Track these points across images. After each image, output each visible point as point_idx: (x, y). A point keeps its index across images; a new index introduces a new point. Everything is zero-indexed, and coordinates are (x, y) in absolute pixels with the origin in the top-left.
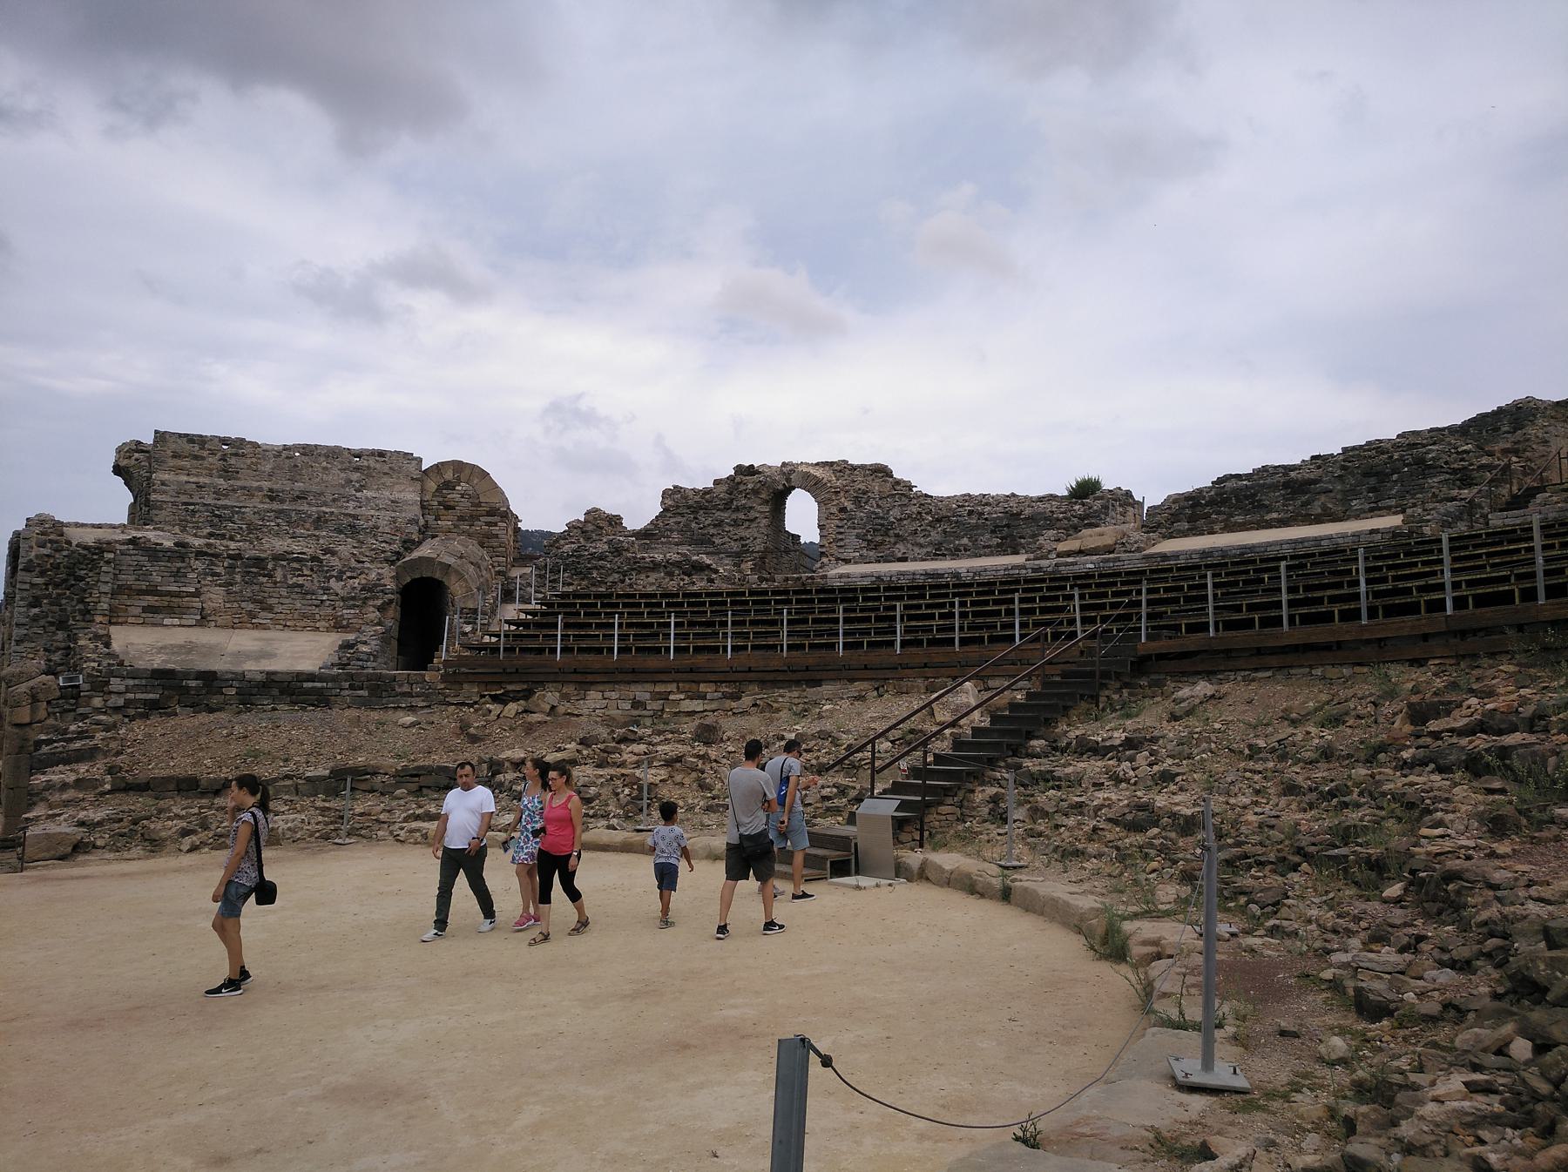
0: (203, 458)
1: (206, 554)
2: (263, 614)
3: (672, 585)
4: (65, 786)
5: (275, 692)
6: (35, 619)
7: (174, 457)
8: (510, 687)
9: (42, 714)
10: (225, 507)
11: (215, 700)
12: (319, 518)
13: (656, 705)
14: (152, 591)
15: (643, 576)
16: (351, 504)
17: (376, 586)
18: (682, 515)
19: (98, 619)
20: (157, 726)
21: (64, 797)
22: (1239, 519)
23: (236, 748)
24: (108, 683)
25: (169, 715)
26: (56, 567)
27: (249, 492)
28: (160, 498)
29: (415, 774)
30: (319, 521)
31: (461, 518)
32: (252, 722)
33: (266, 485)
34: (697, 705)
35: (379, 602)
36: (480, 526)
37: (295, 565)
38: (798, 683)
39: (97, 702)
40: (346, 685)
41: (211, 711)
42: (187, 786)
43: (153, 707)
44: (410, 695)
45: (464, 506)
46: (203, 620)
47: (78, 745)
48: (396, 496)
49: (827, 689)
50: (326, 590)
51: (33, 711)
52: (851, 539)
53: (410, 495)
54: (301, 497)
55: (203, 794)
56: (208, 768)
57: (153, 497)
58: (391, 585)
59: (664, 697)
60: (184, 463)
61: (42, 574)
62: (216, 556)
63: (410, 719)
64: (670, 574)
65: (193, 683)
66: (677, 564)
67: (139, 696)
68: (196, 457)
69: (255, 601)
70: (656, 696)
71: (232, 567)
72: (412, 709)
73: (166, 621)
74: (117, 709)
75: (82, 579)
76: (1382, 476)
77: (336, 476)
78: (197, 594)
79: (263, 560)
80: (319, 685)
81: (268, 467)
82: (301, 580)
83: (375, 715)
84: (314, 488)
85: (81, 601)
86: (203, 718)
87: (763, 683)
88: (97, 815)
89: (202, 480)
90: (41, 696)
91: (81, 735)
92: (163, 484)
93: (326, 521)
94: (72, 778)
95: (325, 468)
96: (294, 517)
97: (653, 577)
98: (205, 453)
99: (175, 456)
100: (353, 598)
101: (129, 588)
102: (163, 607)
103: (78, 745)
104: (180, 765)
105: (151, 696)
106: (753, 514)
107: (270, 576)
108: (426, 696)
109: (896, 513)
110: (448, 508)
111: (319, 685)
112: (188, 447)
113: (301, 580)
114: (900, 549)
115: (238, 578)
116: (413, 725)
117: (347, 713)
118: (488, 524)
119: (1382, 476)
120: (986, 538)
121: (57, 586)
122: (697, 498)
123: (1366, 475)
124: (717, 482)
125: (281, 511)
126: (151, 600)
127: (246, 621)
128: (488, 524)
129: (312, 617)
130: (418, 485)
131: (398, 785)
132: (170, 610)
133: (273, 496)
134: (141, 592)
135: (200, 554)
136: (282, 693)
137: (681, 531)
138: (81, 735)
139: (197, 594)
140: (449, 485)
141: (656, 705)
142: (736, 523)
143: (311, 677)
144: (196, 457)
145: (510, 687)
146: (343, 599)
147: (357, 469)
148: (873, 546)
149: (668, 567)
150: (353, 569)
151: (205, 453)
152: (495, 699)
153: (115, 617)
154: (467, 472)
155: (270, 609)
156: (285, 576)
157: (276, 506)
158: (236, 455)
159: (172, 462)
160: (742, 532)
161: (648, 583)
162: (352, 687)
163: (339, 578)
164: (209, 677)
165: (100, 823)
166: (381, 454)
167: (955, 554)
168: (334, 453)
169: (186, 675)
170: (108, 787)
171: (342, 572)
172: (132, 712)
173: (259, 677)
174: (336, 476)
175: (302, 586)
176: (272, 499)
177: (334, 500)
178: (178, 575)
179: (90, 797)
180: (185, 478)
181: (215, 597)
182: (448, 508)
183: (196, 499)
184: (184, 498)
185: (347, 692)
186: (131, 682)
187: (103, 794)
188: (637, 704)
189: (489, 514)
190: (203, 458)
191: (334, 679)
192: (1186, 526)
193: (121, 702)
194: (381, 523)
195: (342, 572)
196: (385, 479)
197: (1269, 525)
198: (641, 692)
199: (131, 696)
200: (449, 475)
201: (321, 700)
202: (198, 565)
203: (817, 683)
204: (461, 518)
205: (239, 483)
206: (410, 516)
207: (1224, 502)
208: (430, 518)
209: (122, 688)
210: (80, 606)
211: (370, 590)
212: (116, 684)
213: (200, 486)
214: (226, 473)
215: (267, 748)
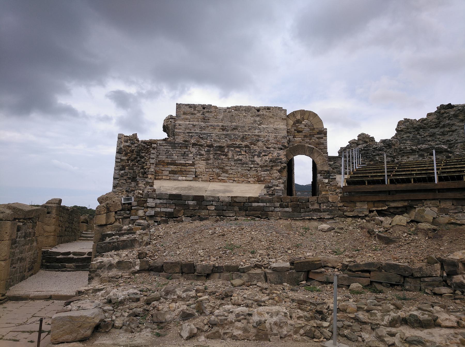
0: (195, 114)
1: (197, 145)
2: (224, 174)
4: (111, 266)
5: (236, 209)
6: (122, 176)
7: (184, 114)
8: (393, 205)
9: (112, 219)
10: (204, 134)
11: (204, 213)
12: (243, 137)
14: (173, 163)
15: (405, 158)
16: (257, 131)
17: (277, 159)
18: (410, 133)
19: (150, 176)
20: (172, 227)
21: (110, 274)
23: (219, 243)
24: (146, 202)
25: (178, 221)
26: (132, 151)
27: (214, 127)
28: (178, 131)
29: (366, 270)
31: (305, 136)
32: (223, 226)
33: (221, 124)
35: (279, 168)
37: (238, 150)
39: (141, 213)
40: (278, 204)
41: (201, 219)
42: (188, 270)
43: (171, 216)
44: (319, 211)
45: (307, 130)
46: (196, 178)
47: (125, 238)
48: (276, 126)
50: (253, 162)
51: (108, 217)
53: (282, 126)
54: (235, 129)
55: (199, 277)
56: (203, 258)
57: (176, 130)
60: (188, 117)
61: (126, 155)
62: (201, 146)
63: (325, 226)
64: (422, 156)
65: (191, 203)
67: (163, 210)
68: (192, 114)
69: (220, 168)
71: (208, 151)
72: (321, 220)
73: (180, 178)
74: (151, 217)
75: (143, 157)
77: (249, 120)
78: (193, 164)
79: (223, 147)
80: (261, 204)
81: (221, 117)
82: (240, 157)
83: (300, 224)
85: (142, 168)
86: (197, 223)
88: (120, 293)
90: (112, 209)
91: (130, 231)
92: (180, 125)
93: (246, 139)
94: (117, 259)
95: (245, 116)
96: (233, 137)
98: (196, 112)
99: (185, 114)
100: (266, 166)
101: (163, 162)
102: (179, 171)
103: (125, 238)
104: (182, 255)
105: (169, 210)
106: (454, 128)
107: (226, 155)
108: (329, 211)
110: (299, 132)
111: (261, 204)
112: (189, 109)
113: (240, 157)
115: (212, 156)
116: (330, 230)
117: (281, 221)
118: (318, 138)
121: (132, 160)
122: (419, 123)
124: (429, 115)
125: (227, 135)
126: (172, 168)
128: (318, 138)
130: (285, 121)
131: (351, 280)
132: (181, 173)
134: (168, 164)
135: (194, 145)
136: (240, 209)
138: (130, 231)
139: (193, 164)
140: (299, 122)
142: (443, 134)
143: (257, 200)
144: (192, 114)
145: (393, 205)
146: (261, 167)
147: (258, 116)
150: (264, 151)
151: (196, 112)
152: (381, 213)
153: (157, 176)
154: (307, 115)
155: (226, 172)
156: (233, 155)
157: (225, 133)
158: (208, 112)
159: (183, 116)
160: (447, 138)
162: (281, 206)
163: (259, 156)
165: (122, 303)
166: (268, 108)
169: (188, 198)
170: (137, 268)
171: (260, 153)
172: (159, 219)
173: (227, 200)
174: (249, 120)
175: (241, 160)
176: (223, 130)
177: (249, 129)
178: (184, 155)
179: (126, 275)
180: (188, 123)
181: (201, 166)
182: (299, 132)
183: (192, 131)
184: (188, 131)
185: (278, 209)
186: (158, 201)
187: (134, 273)
190: (195, 114)
191: (270, 201)
193: (152, 213)
194: (271, 138)
195: (260, 153)
196: (272, 120)
199: (158, 210)
200: (299, 117)
201: (263, 214)
202: (194, 150)
204: (305, 136)
206: (283, 135)
208: (291, 137)
209: (153, 205)
210: (142, 170)
211: (274, 162)
212: (151, 202)
213: (194, 126)
214: (205, 120)
215: (238, 243)
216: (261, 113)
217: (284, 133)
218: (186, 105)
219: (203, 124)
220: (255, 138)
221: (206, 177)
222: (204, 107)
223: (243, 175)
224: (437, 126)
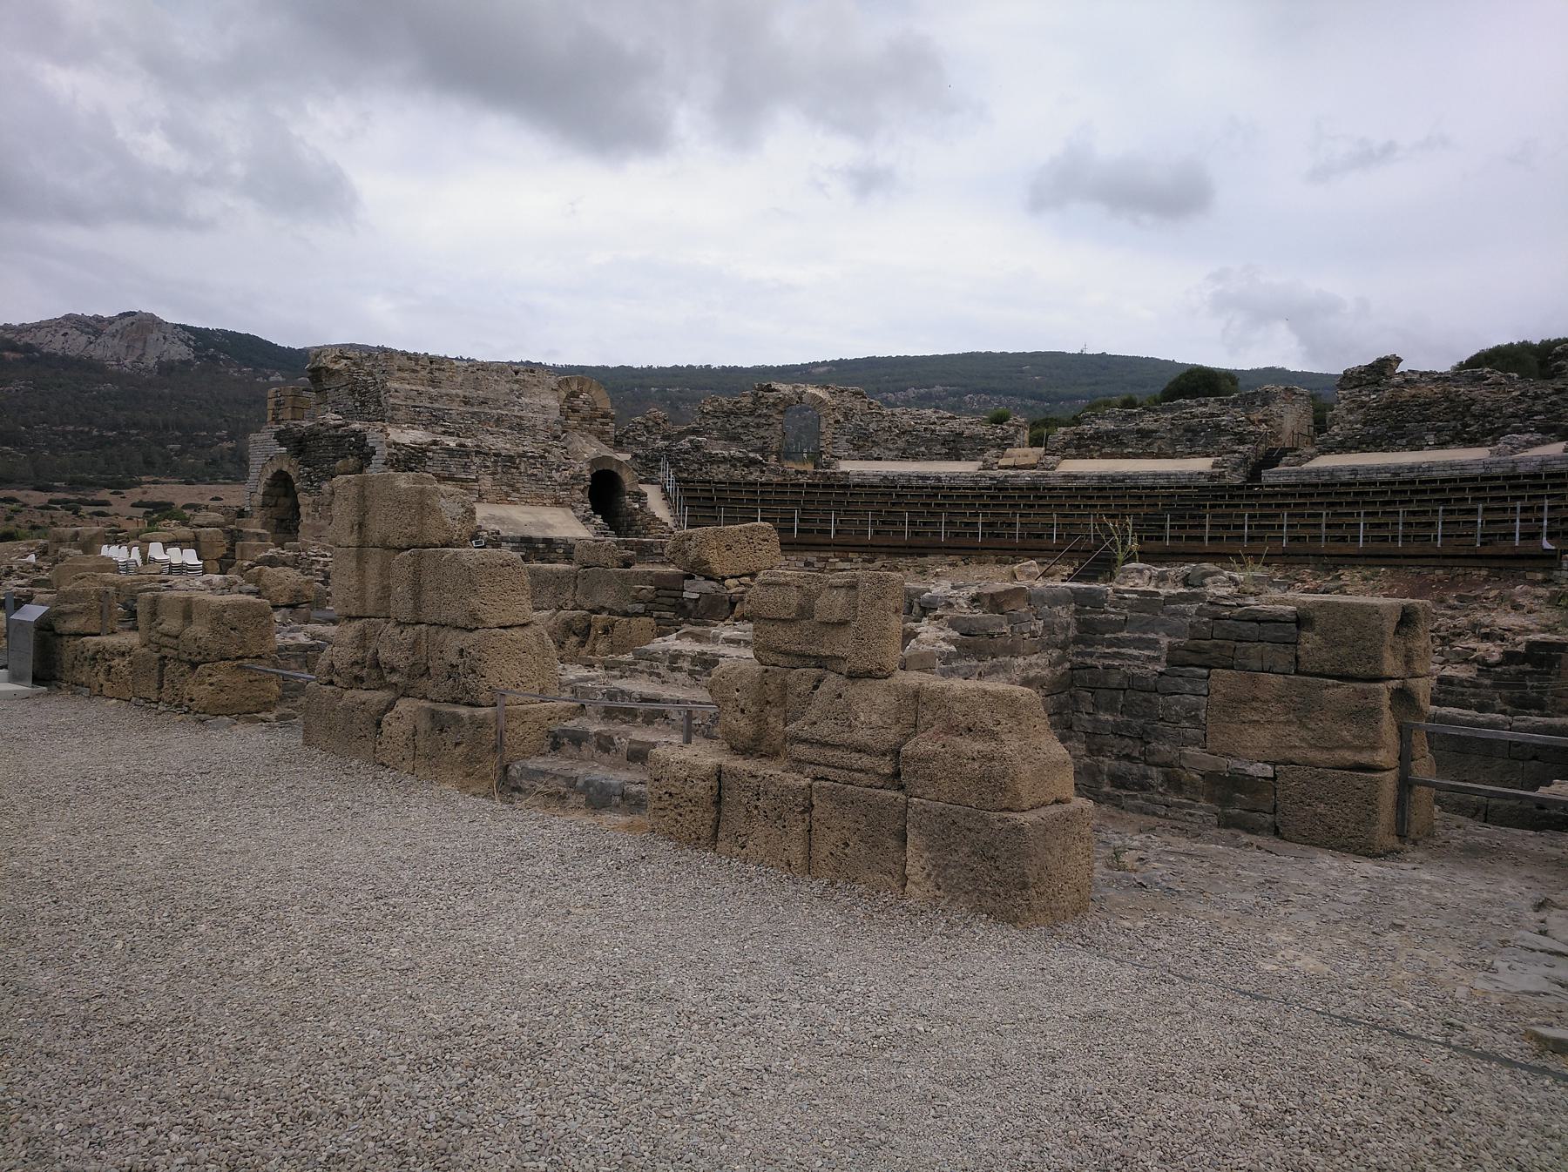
3: (737, 474)
11: (553, 556)
13: (821, 565)
22: (1107, 450)
27: (451, 398)
30: (499, 421)
31: (584, 419)
34: (847, 565)
36: (596, 426)
38: (911, 555)
49: (931, 559)
52: (843, 443)
53: (552, 402)
59: (826, 560)
60: (405, 375)
64: (734, 466)
66: (740, 460)
70: (820, 560)
76: (1195, 433)
77: (504, 387)
78: (476, 480)
84: (491, 396)
87: (889, 554)
89: (421, 388)
97: (722, 468)
106: (771, 420)
109: (873, 426)
110: (574, 411)
112: (408, 363)
114: (876, 451)
119: (1195, 433)
120: (938, 448)
127: (504, 499)
137: (719, 430)
139: (476, 480)
140: (574, 395)
141: (821, 565)
142: (758, 426)
147: (517, 381)
148: (858, 448)
149: (732, 461)
155: (518, 490)
160: (762, 433)
161: (719, 473)
164: (548, 542)
167: (916, 457)
169: (538, 540)
174: (504, 387)
181: (487, 482)
182: (574, 411)
184: (410, 402)
188: (807, 564)
192: (1074, 452)
196: (535, 390)
200: (575, 387)
202: (477, 460)
203: (925, 555)
204: (584, 419)
214: (433, 382)
216: (519, 377)
217: (555, 415)
218: (404, 353)
220: (515, 421)
221: (492, 497)
222: (432, 360)
224: (752, 414)
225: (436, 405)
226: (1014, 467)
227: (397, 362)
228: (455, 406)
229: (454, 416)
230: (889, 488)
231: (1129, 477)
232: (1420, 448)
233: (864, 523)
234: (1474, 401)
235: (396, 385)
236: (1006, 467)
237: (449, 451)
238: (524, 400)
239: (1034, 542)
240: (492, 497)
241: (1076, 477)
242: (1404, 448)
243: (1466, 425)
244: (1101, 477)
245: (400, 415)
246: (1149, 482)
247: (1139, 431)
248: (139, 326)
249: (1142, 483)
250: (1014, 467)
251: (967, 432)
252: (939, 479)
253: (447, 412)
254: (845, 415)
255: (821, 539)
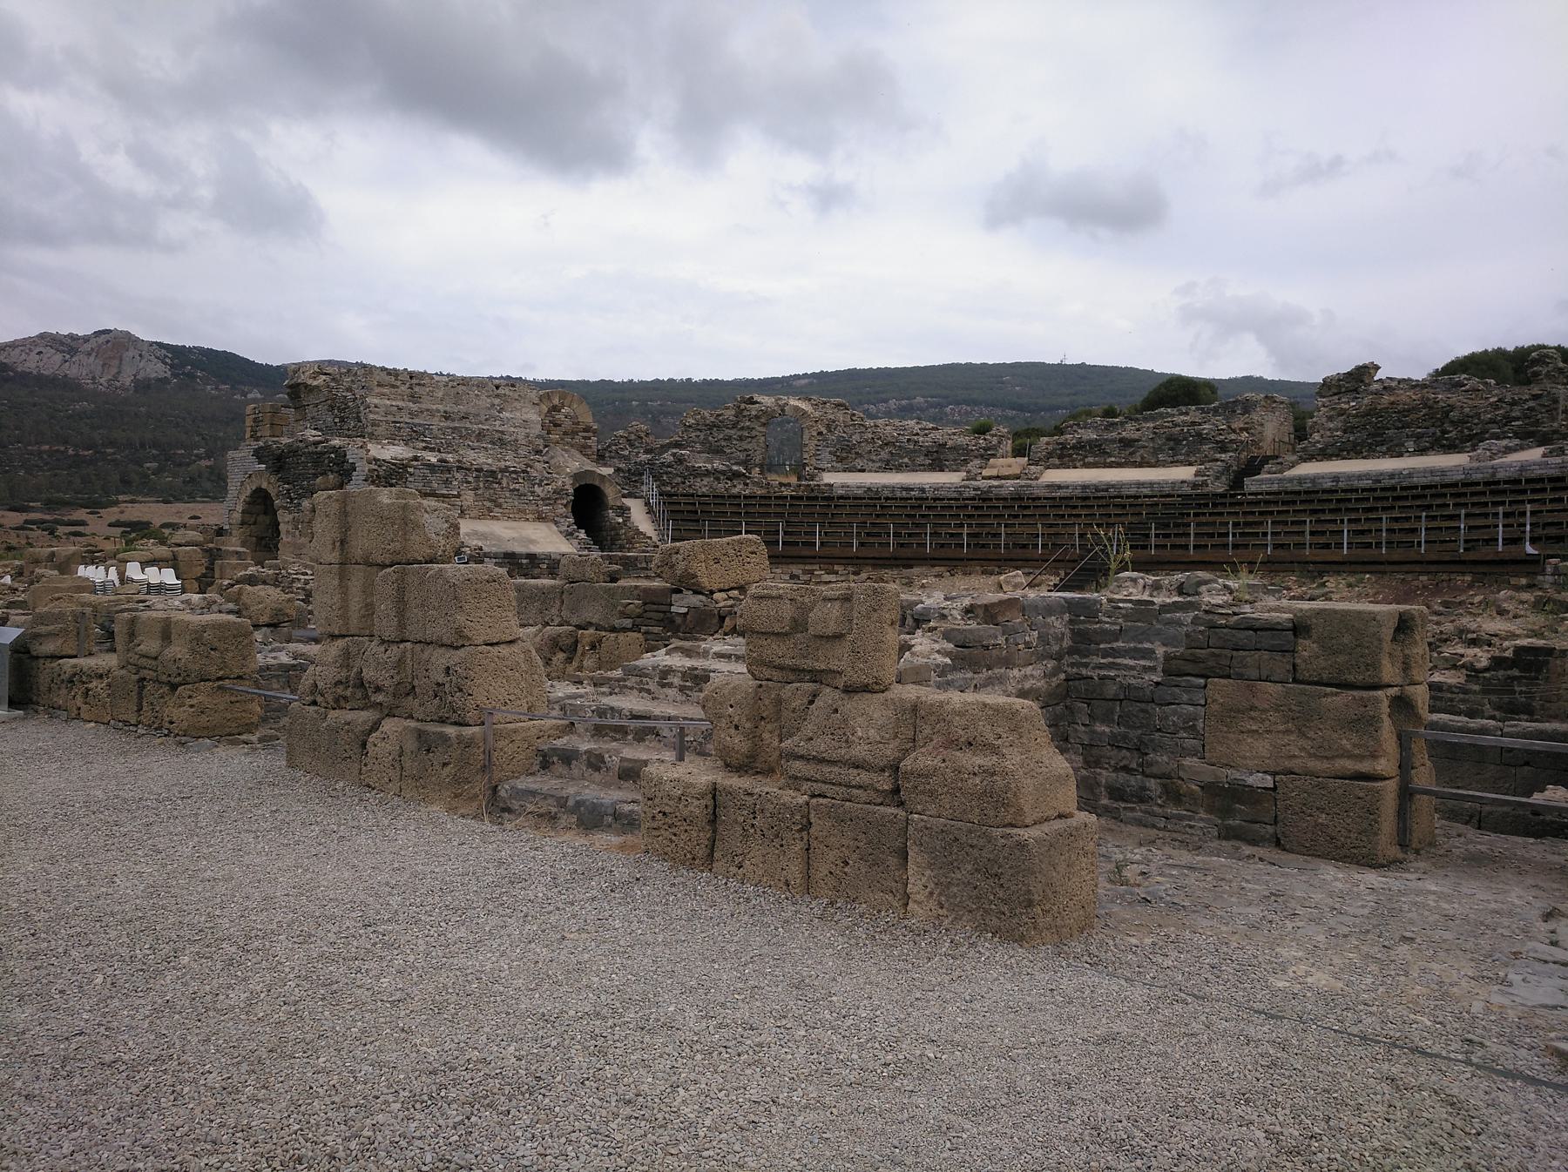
3: (721, 487)
11: (536, 571)
22: (1091, 459)
27: (432, 413)
30: (480, 436)
31: (565, 433)
34: (832, 578)
36: (578, 440)
38: (897, 566)
45: (567, 424)
48: (525, 417)
49: (916, 570)
52: (826, 455)
53: (533, 416)
58: (571, 491)
59: (811, 572)
60: (385, 390)
64: (718, 479)
66: (723, 473)
68: (393, 386)
70: (805, 572)
76: (1177, 441)
77: (485, 402)
78: (458, 496)
81: (440, 394)
84: (473, 411)
87: (875, 566)
89: (400, 404)
97: (706, 481)
106: (754, 433)
109: (856, 438)
110: (556, 425)
114: (859, 463)
119: (1177, 441)
120: (920, 460)
123: (1168, 439)
127: (486, 514)
129: (524, 512)
133: (447, 416)
137: (702, 443)
139: (458, 496)
140: (555, 409)
141: (806, 577)
142: (741, 439)
144: (393, 386)
147: (497, 396)
148: (841, 460)
149: (715, 474)
155: (500, 506)
157: (449, 423)
161: (703, 486)
164: (532, 557)
167: (899, 468)
168: (481, 383)
169: (521, 556)
174: (485, 402)
178: (447, 482)
181: (468, 498)
182: (556, 425)
184: (390, 418)
188: (793, 577)
189: (585, 430)
192: (1057, 462)
197: (1110, 466)
198: (796, 570)
200: (556, 401)
202: (458, 475)
204: (565, 433)
205: (424, 406)
207: (1083, 447)
214: (414, 398)
216: (501, 391)
217: (537, 429)
218: (383, 369)
219: (414, 407)
220: (497, 435)
221: (475, 513)
222: (412, 375)
223: (520, 511)
225: (416, 421)
226: (998, 477)
227: (377, 377)
228: (435, 421)
229: (435, 431)
230: (873, 499)
231: (1113, 486)
232: (1400, 455)
233: (849, 535)
234: (1452, 407)
235: (376, 401)
236: (990, 478)
237: (431, 467)
238: (505, 414)
239: (1019, 552)
240: (475, 513)
241: (1060, 487)
242: (1384, 455)
243: (1444, 432)
244: (1084, 487)
245: (380, 430)
246: (1133, 491)
247: (1121, 440)
248: (113, 344)
249: (1125, 492)
250: (998, 477)
251: (950, 443)
252: (923, 490)
253: (428, 427)
254: (828, 427)
255: (806, 552)
